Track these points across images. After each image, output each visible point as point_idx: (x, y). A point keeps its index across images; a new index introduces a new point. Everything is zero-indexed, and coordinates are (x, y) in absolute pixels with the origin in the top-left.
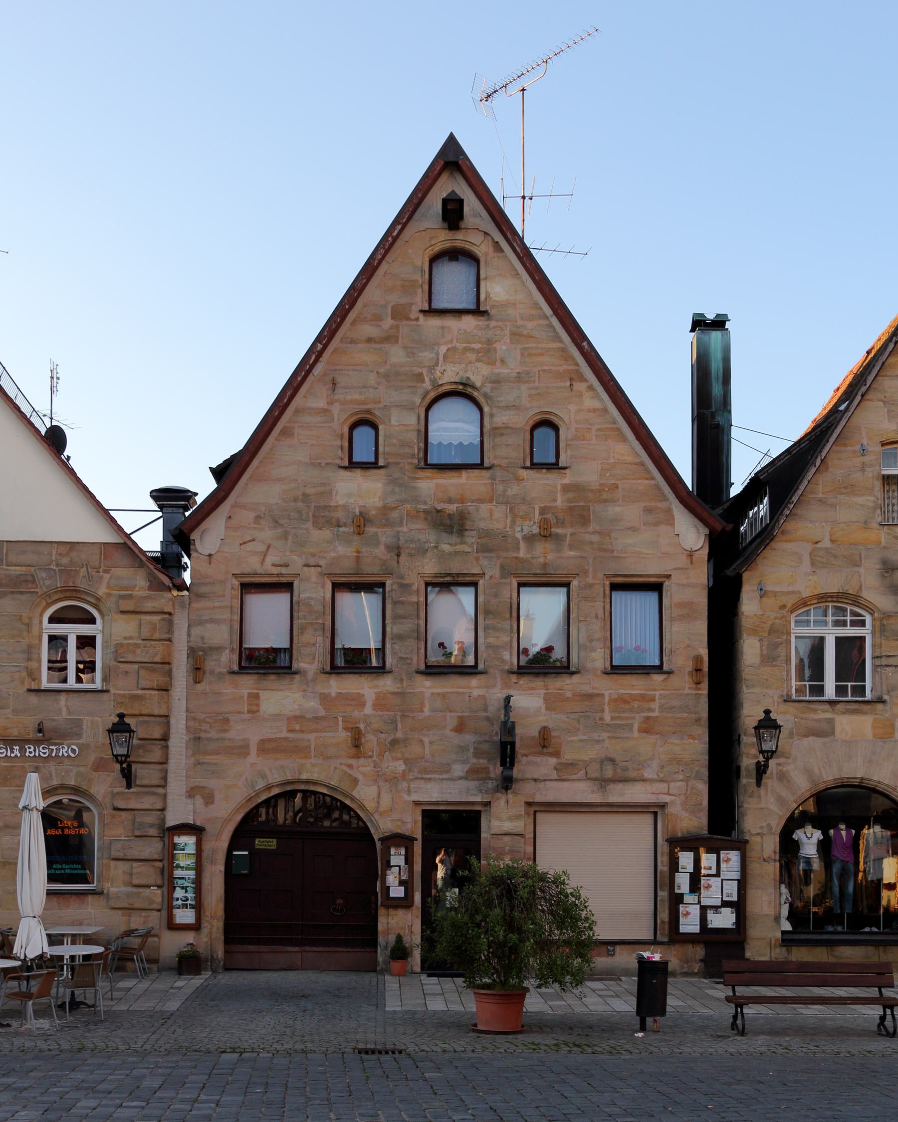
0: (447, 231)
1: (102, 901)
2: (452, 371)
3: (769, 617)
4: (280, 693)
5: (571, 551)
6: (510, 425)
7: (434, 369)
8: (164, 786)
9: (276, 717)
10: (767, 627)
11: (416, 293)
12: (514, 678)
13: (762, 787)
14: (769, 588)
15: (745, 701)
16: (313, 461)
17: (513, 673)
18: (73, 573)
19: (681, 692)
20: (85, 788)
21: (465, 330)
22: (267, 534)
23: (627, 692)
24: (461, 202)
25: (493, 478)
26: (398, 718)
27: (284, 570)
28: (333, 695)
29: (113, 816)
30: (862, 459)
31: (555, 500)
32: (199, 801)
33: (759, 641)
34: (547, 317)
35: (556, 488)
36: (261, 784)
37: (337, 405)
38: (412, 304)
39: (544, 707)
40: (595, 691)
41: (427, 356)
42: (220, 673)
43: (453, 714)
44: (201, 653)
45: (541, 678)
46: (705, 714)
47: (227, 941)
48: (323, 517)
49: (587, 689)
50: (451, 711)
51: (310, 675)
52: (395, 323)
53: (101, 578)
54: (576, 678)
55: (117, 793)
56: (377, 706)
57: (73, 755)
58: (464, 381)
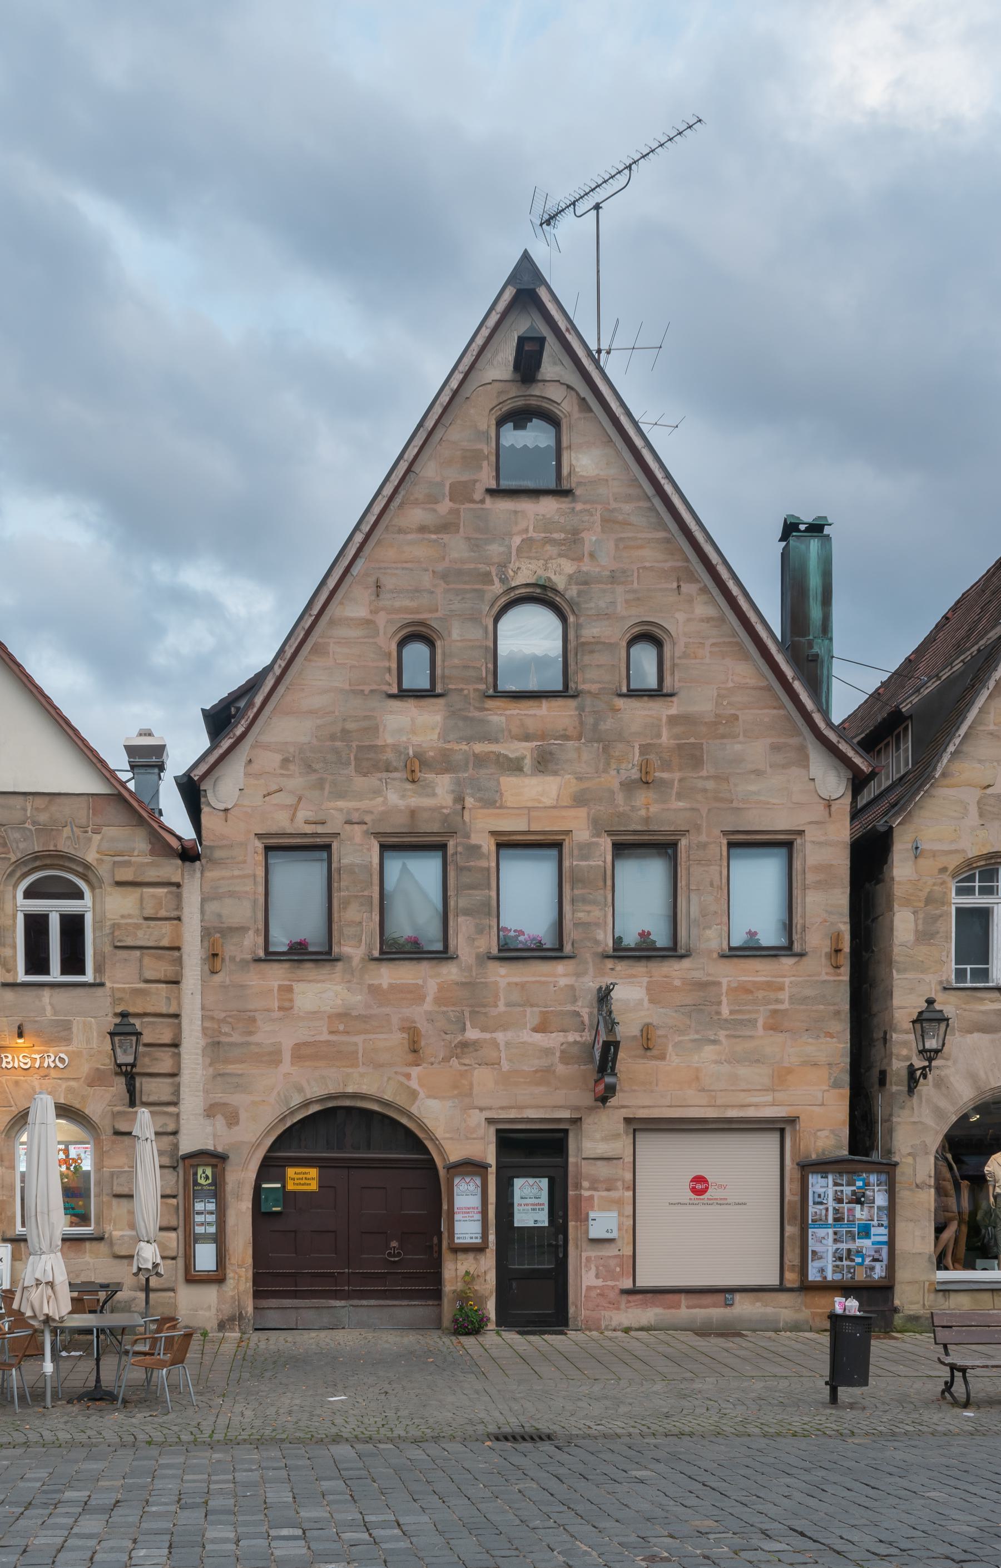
1: (102, 1247)
2: (528, 569)
3: (925, 883)
4: (319, 985)
5: (680, 801)
6: (602, 640)
7: (505, 566)
8: (175, 1104)
9: (314, 1015)
10: (923, 895)
11: (481, 468)
12: (609, 964)
13: (915, 1097)
14: (924, 846)
15: (895, 989)
16: (353, 688)
17: (608, 957)
18: (54, 833)
19: (817, 978)
20: (78, 1106)
21: (543, 515)
22: (297, 782)
23: (750, 979)
25: (581, 709)
26: (467, 1014)
27: (320, 829)
28: (385, 986)
31: (659, 736)
32: (220, 1121)
33: (914, 913)
34: (649, 498)
35: (661, 720)
36: (296, 1100)
37: (382, 614)
38: (475, 481)
39: (646, 999)
40: (710, 978)
41: (495, 550)
42: (242, 960)
43: (535, 1009)
44: (218, 935)
45: (643, 963)
46: (847, 1007)
48: (368, 759)
49: (698, 975)
50: (532, 1006)
51: (356, 961)
52: (456, 506)
53: (90, 839)
54: (686, 963)
55: (119, 1113)
56: (438, 1001)
57: (61, 1066)
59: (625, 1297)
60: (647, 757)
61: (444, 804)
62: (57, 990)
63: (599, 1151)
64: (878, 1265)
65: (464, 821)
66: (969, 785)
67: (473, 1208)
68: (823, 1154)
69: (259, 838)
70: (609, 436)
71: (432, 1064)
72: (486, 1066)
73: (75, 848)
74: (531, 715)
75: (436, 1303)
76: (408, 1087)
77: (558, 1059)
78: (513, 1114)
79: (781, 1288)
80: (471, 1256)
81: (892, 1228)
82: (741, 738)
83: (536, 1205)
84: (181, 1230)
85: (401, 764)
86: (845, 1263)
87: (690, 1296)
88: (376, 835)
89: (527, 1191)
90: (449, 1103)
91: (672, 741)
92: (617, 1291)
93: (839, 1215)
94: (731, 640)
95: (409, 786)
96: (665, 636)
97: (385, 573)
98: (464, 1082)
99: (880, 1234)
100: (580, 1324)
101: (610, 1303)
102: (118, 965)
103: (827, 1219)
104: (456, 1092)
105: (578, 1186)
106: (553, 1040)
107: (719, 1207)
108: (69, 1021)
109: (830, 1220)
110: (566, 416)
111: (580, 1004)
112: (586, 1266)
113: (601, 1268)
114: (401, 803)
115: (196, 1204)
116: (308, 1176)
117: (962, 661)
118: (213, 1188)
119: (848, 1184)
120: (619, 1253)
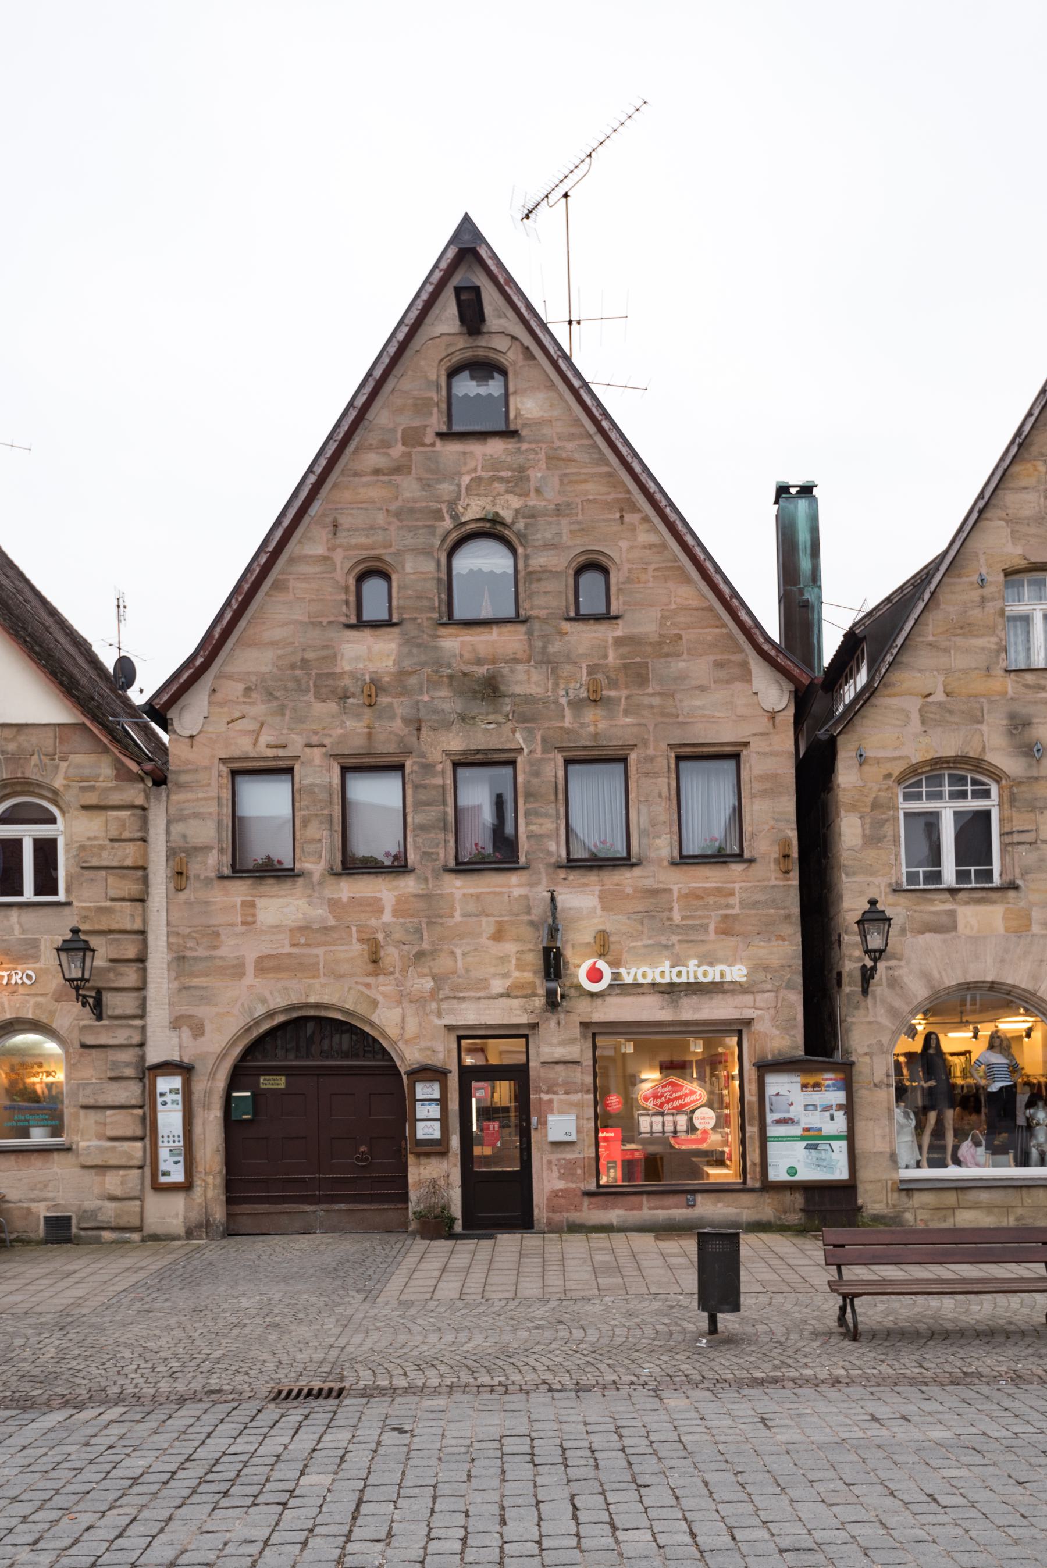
0: (466, 337)
2: (477, 505)
3: (871, 789)
4: (281, 900)
6: (549, 568)
7: (455, 504)
8: (142, 1017)
9: (276, 928)
10: (869, 800)
11: (431, 414)
12: (562, 873)
13: (869, 997)
14: (869, 753)
15: (844, 892)
17: (560, 867)
18: (22, 761)
19: (766, 883)
20: (45, 1021)
22: (259, 709)
23: (701, 885)
24: (477, 290)
25: (530, 633)
26: (424, 926)
27: (281, 753)
28: (345, 899)
29: (81, 1055)
30: (980, 591)
31: (606, 657)
32: (186, 1032)
33: (860, 818)
34: (590, 436)
35: (607, 642)
36: (260, 1011)
37: (339, 550)
38: (426, 426)
39: (599, 906)
40: (661, 886)
41: (446, 489)
42: (207, 878)
43: (490, 919)
44: (183, 855)
45: (595, 872)
46: (796, 910)
47: (230, 1201)
48: (326, 686)
49: (649, 883)
50: (487, 916)
51: (316, 877)
52: (407, 450)
53: (57, 767)
54: (637, 872)
55: (85, 1027)
56: (396, 913)
57: (28, 982)
58: (490, 517)
66: (910, 694)
82: (685, 656)
84: (147, 1141)
87: (651, 1197)
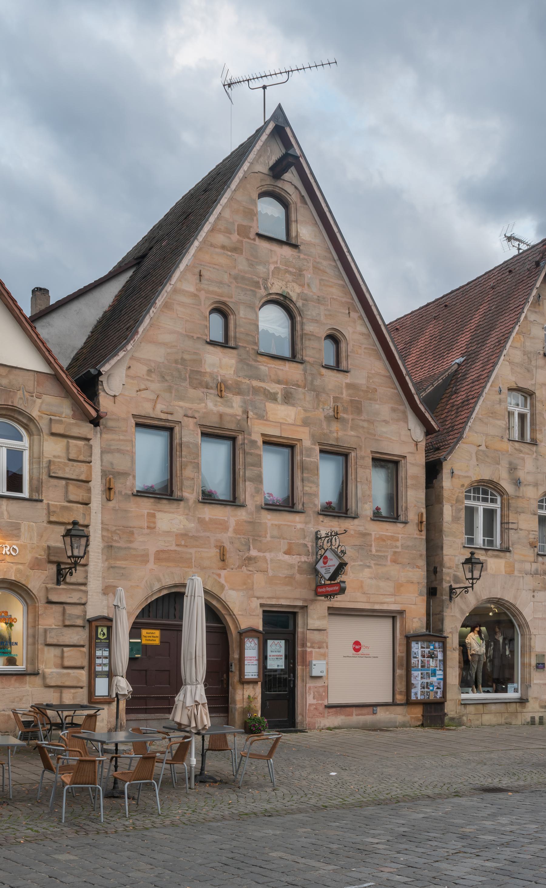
0: (271, 178)
1: (37, 680)
2: (278, 285)
4: (171, 515)
5: (352, 431)
6: (315, 334)
7: (266, 280)
8: (85, 584)
9: (168, 533)
10: (455, 497)
13: (453, 602)
15: (444, 545)
16: (188, 334)
18: (11, 393)
19: (412, 536)
20: (24, 583)
21: (285, 256)
22: (156, 386)
23: (384, 533)
25: (305, 371)
26: (251, 541)
27: (170, 417)
28: (207, 519)
29: (46, 608)
30: (499, 396)
31: (342, 394)
34: (335, 260)
35: (342, 385)
36: (157, 586)
37: (203, 292)
41: (261, 269)
42: (126, 494)
43: (285, 541)
44: (111, 476)
45: (336, 519)
48: (196, 379)
49: (361, 529)
50: (284, 539)
51: (191, 502)
52: (241, 239)
53: (35, 402)
54: (356, 521)
55: (52, 588)
56: (236, 531)
57: (14, 554)
58: (285, 294)
59: (327, 710)
60: (337, 404)
61: (238, 414)
62: (11, 501)
63: (316, 625)
64: (439, 691)
65: (248, 425)
66: (472, 444)
67: (253, 657)
68: (416, 630)
69: (133, 417)
70: (316, 221)
71: (232, 569)
72: (260, 573)
73: (25, 406)
74: (280, 369)
75: (225, 715)
76: (219, 582)
77: (296, 571)
78: (274, 602)
79: (394, 704)
80: (251, 686)
81: (445, 671)
82: (378, 402)
83: (278, 656)
84: (86, 668)
85: (214, 385)
86: (426, 690)
87: (358, 709)
88: (201, 426)
89: (274, 647)
90: (241, 593)
91: (347, 397)
92: (323, 706)
93: (423, 664)
94: (373, 347)
95: (219, 399)
96: (342, 339)
97: (204, 268)
98: (249, 581)
99: (440, 673)
100: (305, 726)
101: (320, 713)
102: (51, 488)
103: (418, 666)
104: (245, 587)
105: (304, 645)
106: (294, 560)
107: (366, 659)
108: (19, 523)
109: (420, 667)
110: (293, 203)
111: (307, 539)
112: (309, 692)
113: (316, 693)
114: (215, 409)
115: (97, 652)
116: (154, 635)
117: (442, 379)
118: (108, 641)
119: (427, 648)
120: (324, 684)
